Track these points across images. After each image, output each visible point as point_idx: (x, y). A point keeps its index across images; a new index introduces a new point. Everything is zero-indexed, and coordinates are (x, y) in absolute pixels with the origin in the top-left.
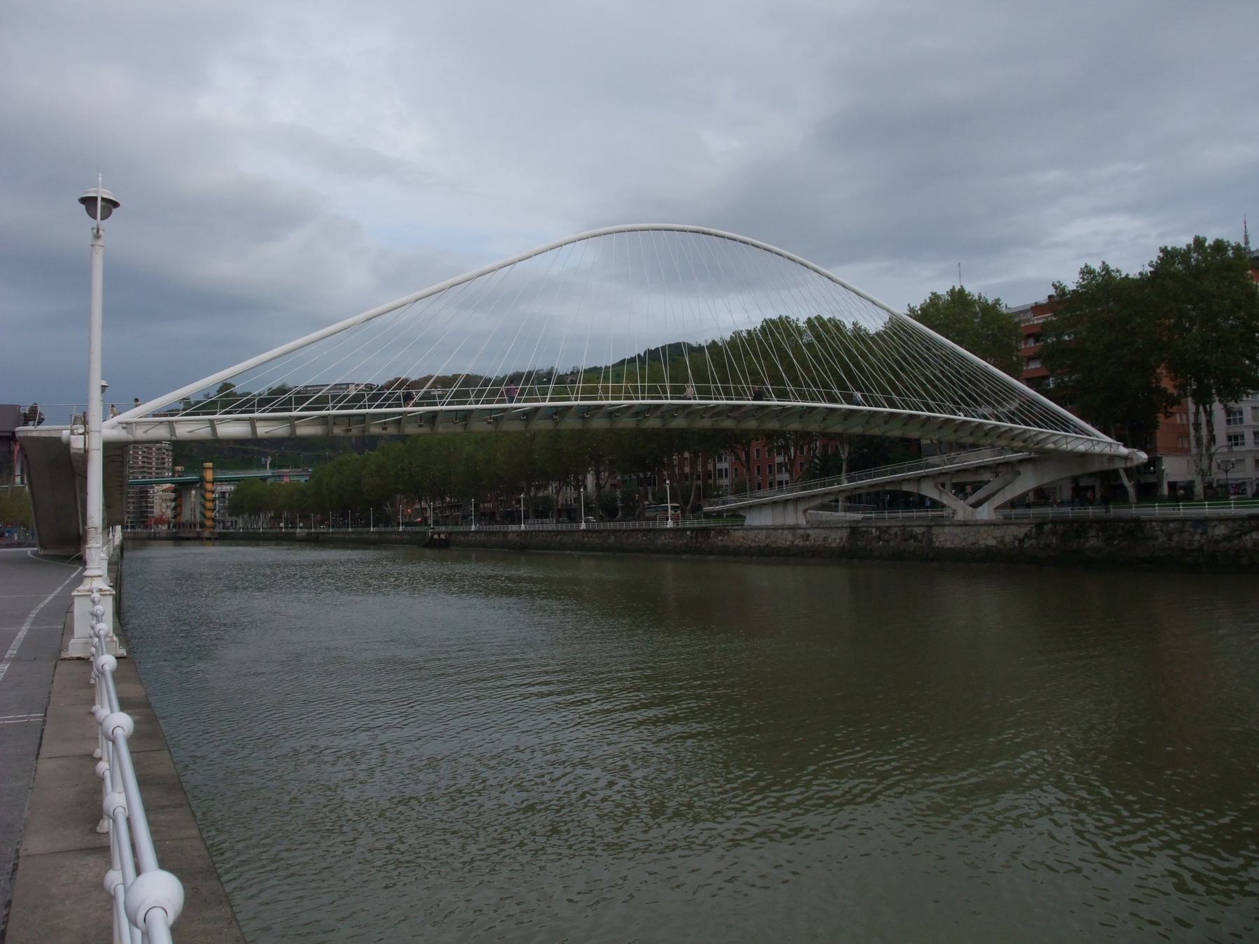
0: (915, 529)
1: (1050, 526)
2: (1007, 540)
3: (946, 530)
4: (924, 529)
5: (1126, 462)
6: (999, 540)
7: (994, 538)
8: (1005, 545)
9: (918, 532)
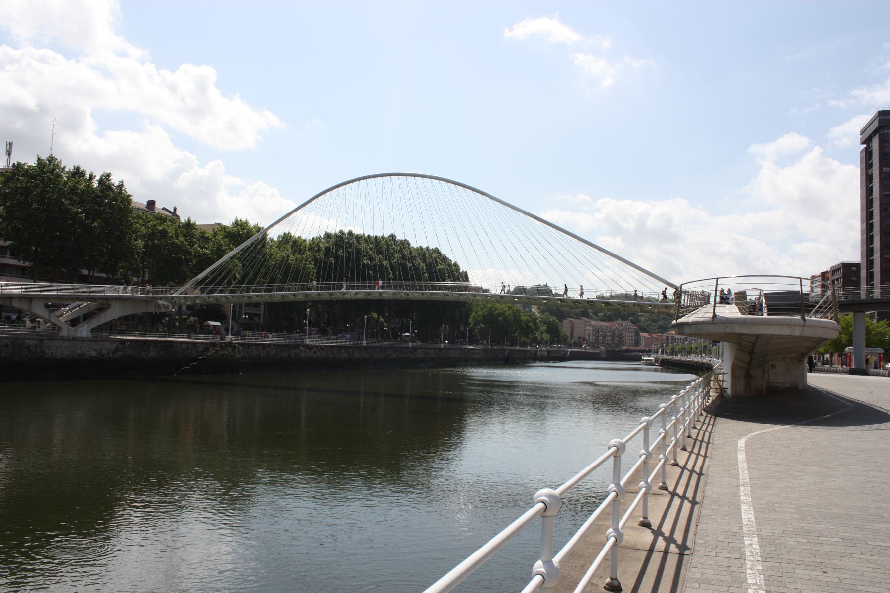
0: (26, 341)
1: (129, 343)
2: (104, 352)
3: (57, 343)
4: (35, 342)
5: (166, 309)
6: (99, 352)
7: (95, 350)
8: (103, 356)
9: (31, 344)
